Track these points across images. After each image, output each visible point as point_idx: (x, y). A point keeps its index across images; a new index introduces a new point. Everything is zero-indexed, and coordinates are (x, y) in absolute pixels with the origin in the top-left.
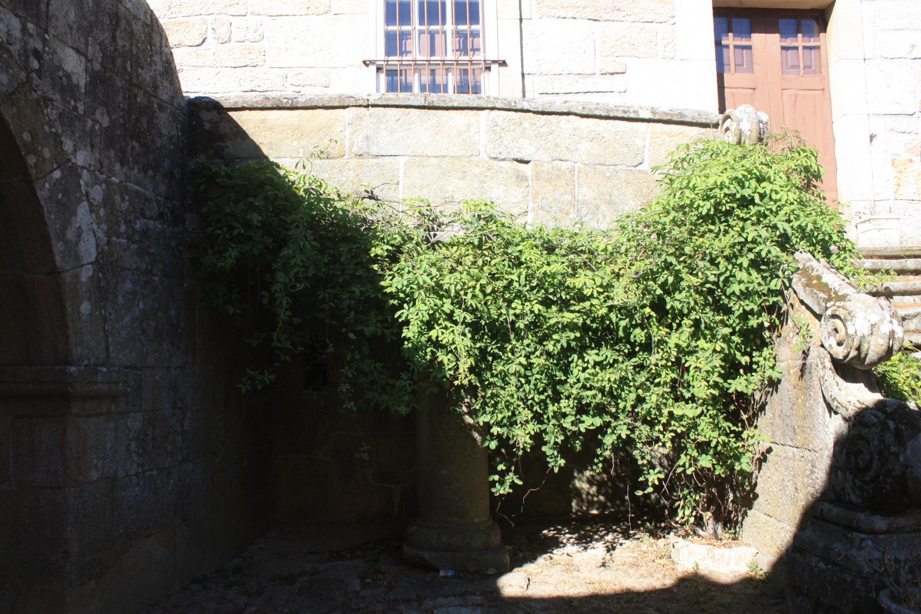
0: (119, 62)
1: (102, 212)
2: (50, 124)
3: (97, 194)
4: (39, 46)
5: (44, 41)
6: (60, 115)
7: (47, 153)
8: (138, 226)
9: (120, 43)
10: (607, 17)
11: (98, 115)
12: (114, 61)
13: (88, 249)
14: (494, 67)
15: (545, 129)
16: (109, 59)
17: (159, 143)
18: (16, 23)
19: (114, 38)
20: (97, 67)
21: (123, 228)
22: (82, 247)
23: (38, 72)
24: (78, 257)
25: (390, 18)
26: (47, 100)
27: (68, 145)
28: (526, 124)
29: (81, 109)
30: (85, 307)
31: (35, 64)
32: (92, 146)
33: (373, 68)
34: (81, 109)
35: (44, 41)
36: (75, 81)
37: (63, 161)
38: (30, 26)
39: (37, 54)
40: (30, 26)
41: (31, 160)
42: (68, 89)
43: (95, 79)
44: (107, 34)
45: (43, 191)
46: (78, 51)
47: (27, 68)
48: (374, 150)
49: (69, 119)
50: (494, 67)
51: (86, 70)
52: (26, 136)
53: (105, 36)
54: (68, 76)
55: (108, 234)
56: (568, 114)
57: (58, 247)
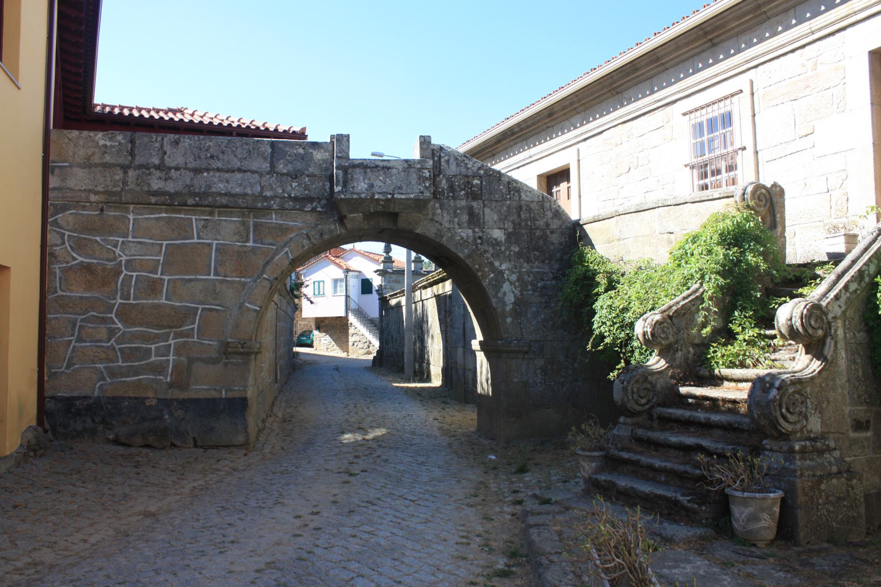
0: (523, 224)
1: (517, 284)
2: (488, 258)
3: (514, 277)
4: (481, 234)
5: (483, 232)
6: (492, 255)
7: (486, 270)
8: (539, 285)
9: (523, 216)
10: (802, 95)
11: (512, 248)
12: (520, 224)
13: (510, 299)
14: (740, 152)
15: (678, 214)
16: (517, 225)
17: (552, 248)
19: (519, 216)
20: (510, 230)
21: (530, 287)
22: (506, 299)
23: (481, 244)
24: (504, 302)
26: (485, 251)
27: (497, 264)
28: (671, 212)
29: (503, 248)
30: (509, 320)
31: (480, 241)
34: (503, 248)
35: (483, 232)
37: (493, 269)
38: (477, 230)
39: (480, 238)
40: (477, 230)
41: (479, 274)
42: (496, 243)
43: (509, 236)
45: (485, 283)
46: (500, 228)
47: (476, 244)
49: (496, 255)
50: (740, 152)
52: (477, 267)
54: (496, 239)
55: (521, 291)
56: (686, 203)
57: (494, 301)
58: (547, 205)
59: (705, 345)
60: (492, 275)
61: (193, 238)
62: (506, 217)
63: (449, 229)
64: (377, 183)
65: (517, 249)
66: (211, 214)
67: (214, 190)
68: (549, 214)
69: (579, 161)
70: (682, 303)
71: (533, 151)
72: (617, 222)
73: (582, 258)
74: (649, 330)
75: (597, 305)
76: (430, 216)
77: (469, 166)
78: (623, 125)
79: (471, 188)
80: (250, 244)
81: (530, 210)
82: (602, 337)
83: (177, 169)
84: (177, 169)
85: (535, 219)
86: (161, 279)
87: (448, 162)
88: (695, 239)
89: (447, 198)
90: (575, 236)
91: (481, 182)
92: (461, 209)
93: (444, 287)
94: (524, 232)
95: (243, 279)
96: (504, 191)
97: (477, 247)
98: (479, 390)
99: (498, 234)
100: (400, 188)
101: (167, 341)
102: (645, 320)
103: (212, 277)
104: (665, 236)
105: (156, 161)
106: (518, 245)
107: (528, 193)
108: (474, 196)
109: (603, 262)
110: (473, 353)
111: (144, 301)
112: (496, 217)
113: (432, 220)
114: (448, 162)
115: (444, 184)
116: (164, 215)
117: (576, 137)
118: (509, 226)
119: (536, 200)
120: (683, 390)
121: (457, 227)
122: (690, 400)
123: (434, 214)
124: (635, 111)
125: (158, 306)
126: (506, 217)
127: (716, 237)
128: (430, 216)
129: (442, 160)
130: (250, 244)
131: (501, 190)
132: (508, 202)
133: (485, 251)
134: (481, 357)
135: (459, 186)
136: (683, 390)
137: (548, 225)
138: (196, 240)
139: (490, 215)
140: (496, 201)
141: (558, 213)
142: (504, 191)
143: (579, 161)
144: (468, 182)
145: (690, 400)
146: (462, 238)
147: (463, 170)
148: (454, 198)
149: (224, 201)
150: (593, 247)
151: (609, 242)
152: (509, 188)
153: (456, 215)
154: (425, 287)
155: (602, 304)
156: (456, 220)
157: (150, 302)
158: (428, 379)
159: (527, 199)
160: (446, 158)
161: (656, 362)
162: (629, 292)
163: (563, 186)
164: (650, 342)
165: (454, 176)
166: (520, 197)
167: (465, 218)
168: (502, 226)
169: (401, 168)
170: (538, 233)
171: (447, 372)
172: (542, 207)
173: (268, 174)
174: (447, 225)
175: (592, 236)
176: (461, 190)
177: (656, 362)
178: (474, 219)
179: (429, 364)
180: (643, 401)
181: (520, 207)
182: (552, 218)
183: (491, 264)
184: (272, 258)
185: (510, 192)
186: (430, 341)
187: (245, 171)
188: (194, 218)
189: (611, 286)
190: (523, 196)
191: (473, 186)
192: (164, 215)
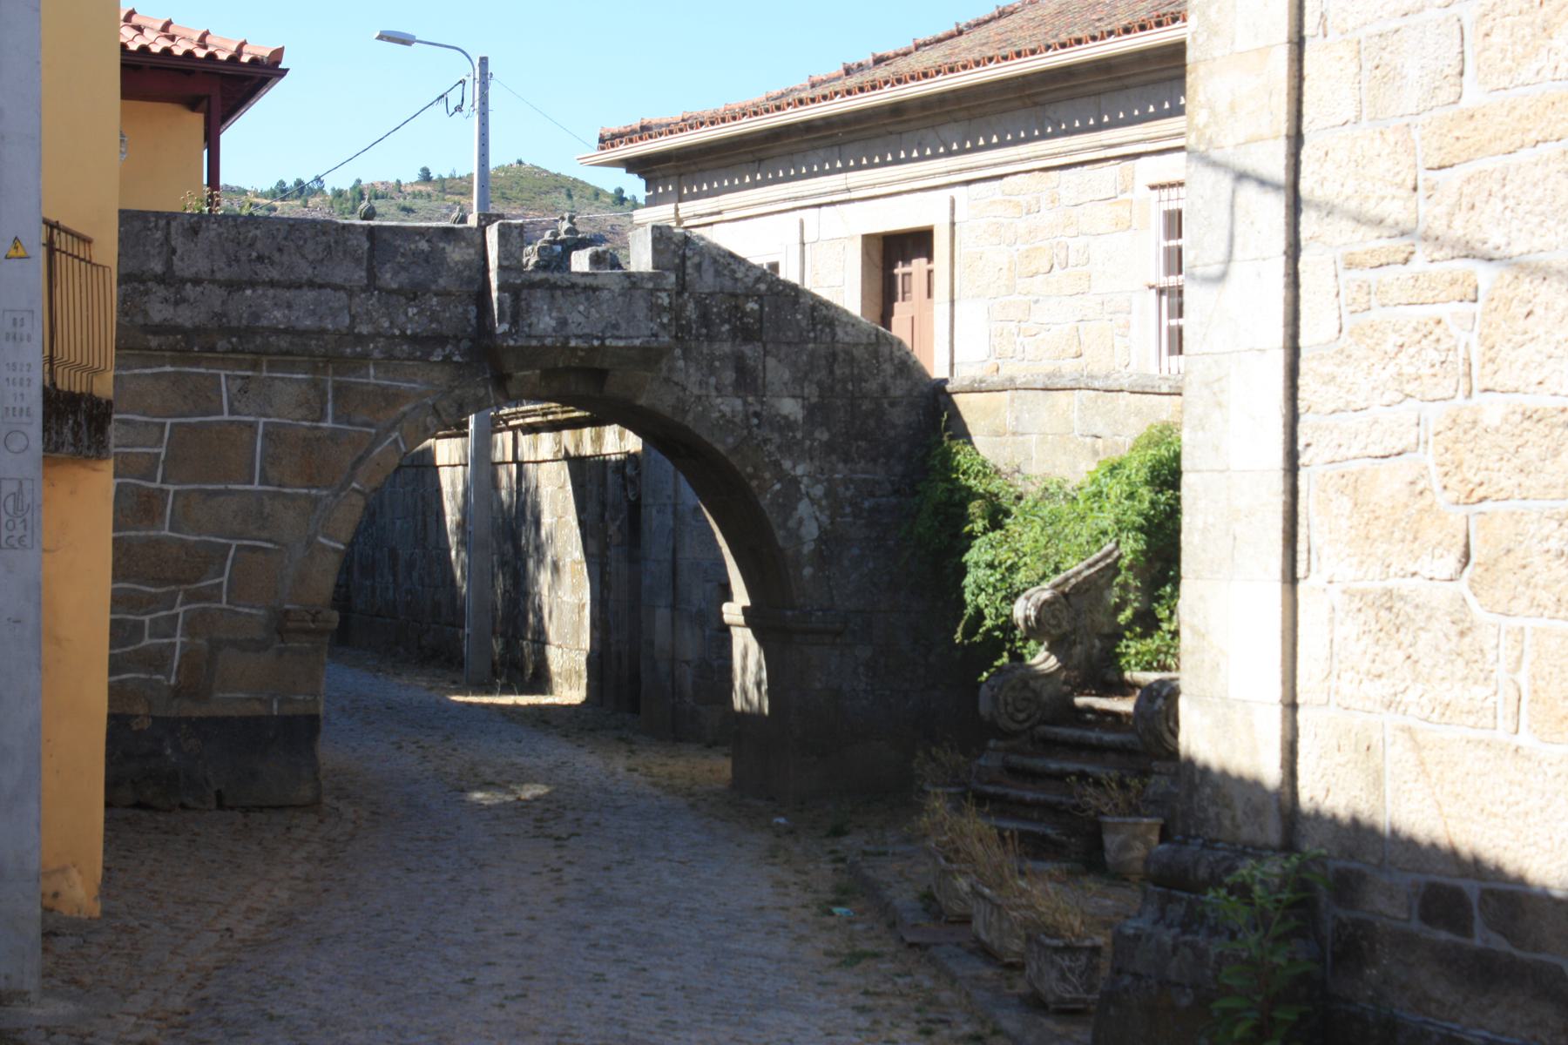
0: (838, 387)
1: (824, 503)
2: (770, 454)
3: (818, 491)
4: (758, 408)
5: (763, 403)
6: (779, 447)
7: (767, 475)
8: (866, 505)
9: (838, 372)
11: (817, 434)
12: (832, 389)
13: (811, 531)
17: (892, 433)
18: (738, 403)
19: (831, 372)
20: (814, 400)
21: (848, 510)
22: (803, 531)
23: (758, 426)
24: (799, 538)
25: (1169, 236)
26: (766, 441)
27: (787, 464)
29: (799, 435)
30: (807, 571)
31: (755, 421)
32: (812, 459)
33: (1154, 291)
34: (799, 435)
35: (763, 403)
36: (792, 418)
37: (781, 475)
38: (750, 399)
39: (756, 414)
40: (750, 399)
41: (754, 483)
42: (787, 425)
43: (811, 411)
44: (824, 372)
45: (765, 500)
46: (794, 397)
47: (749, 427)
48: (1020, 429)
49: (787, 448)
51: (803, 407)
52: (749, 470)
53: (822, 374)
54: (786, 418)
55: (832, 518)
57: (780, 534)
58: (885, 350)
59: (1117, 635)
60: (778, 487)
62: (806, 374)
63: (699, 398)
64: (575, 318)
65: (825, 436)
66: (255, 366)
67: (264, 323)
68: (888, 368)
69: (953, 224)
70: (1086, 573)
71: (855, 178)
72: (1012, 401)
73: (948, 456)
74: (1032, 613)
75: (971, 557)
76: (664, 373)
77: (739, 275)
78: (1044, 174)
79: (741, 319)
80: (328, 424)
81: (852, 360)
82: (979, 615)
83: (197, 281)
84: (197, 281)
85: (861, 379)
86: (162, 490)
87: (698, 266)
88: (1114, 469)
89: (697, 339)
90: (935, 410)
91: (762, 307)
92: (722, 359)
93: (598, 440)
94: (839, 403)
95: (314, 492)
96: (804, 323)
97: (750, 432)
98: (738, 703)
99: (790, 407)
100: (616, 326)
101: (172, 608)
102: (1028, 599)
103: (256, 486)
104: (1089, 440)
105: (157, 267)
106: (829, 430)
107: (849, 328)
108: (746, 334)
109: (986, 471)
110: (725, 629)
111: (133, 533)
112: (787, 376)
113: (667, 380)
114: (698, 266)
115: (691, 311)
116: (168, 369)
117: (949, 173)
118: (811, 391)
119: (864, 340)
120: (1080, 701)
121: (714, 393)
122: (1089, 716)
123: (671, 370)
124: (1066, 153)
125: (158, 542)
126: (806, 374)
127: (1144, 473)
128: (664, 373)
129: (689, 263)
130: (328, 424)
131: (798, 322)
132: (811, 346)
133: (766, 441)
134: (744, 644)
135: (719, 314)
136: (1080, 701)
137: (885, 389)
138: (226, 417)
139: (776, 372)
140: (789, 344)
141: (907, 367)
142: (804, 323)
143: (953, 224)
144: (737, 307)
145: (1089, 716)
146: (724, 415)
147: (728, 283)
148: (711, 338)
149: (284, 344)
150: (963, 434)
151: (997, 434)
152: (813, 318)
153: (712, 371)
154: (533, 429)
155: (977, 554)
156: (713, 380)
157: (142, 533)
158: (540, 680)
159: (847, 339)
160: (696, 259)
161: (1042, 659)
162: (1024, 534)
163: (918, 265)
164: (1036, 630)
165: (711, 295)
166: (834, 335)
167: (729, 376)
168: (798, 392)
169: (617, 289)
170: (866, 406)
171: (598, 664)
172: (876, 355)
173: (363, 290)
174: (696, 391)
175: (968, 417)
176: (724, 322)
177: (1042, 659)
178: (747, 380)
179: (541, 640)
180: (1021, 716)
181: (834, 355)
182: (894, 377)
183: (777, 464)
184: (369, 451)
185: (814, 325)
186: (545, 578)
187: (321, 286)
188: (223, 373)
189: (997, 516)
190: (840, 333)
191: (745, 314)
192: (168, 369)
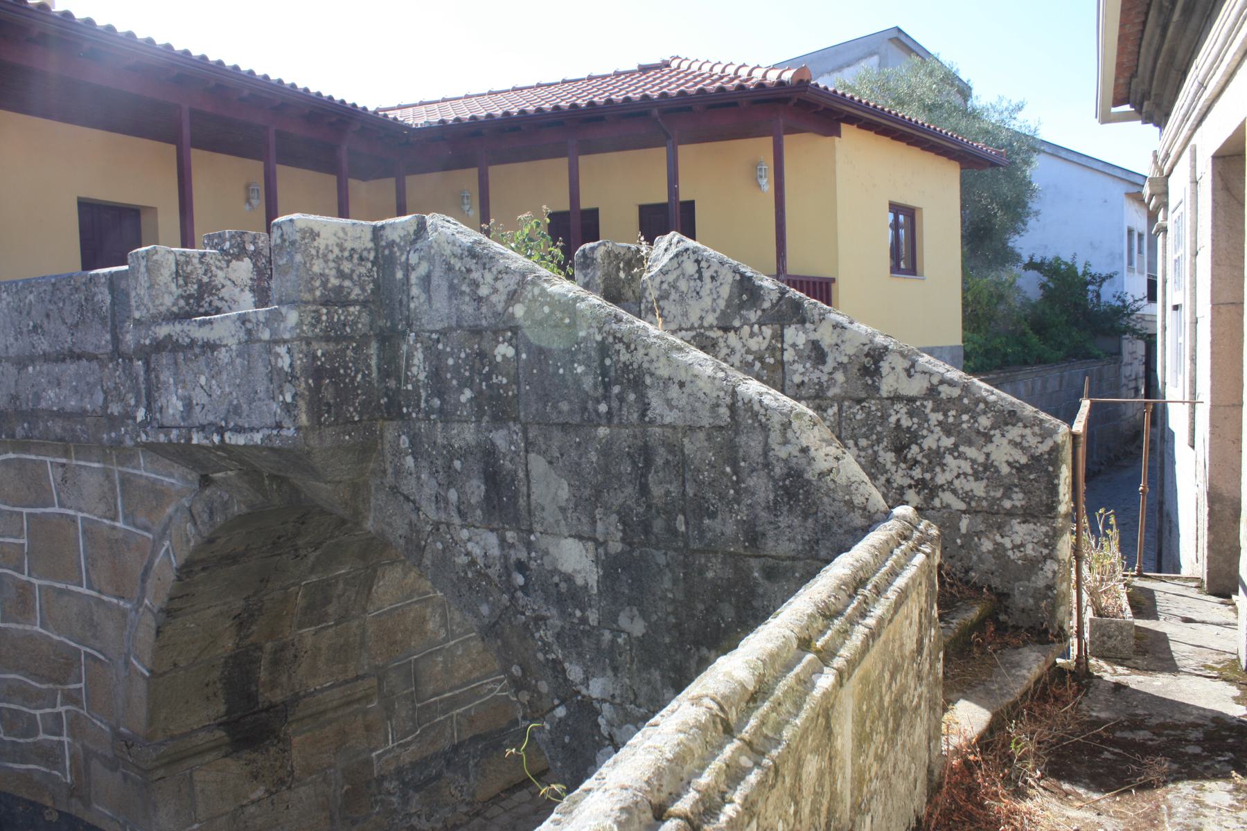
0: (658, 525)
4: (523, 555)
5: (529, 546)
6: (558, 636)
7: (544, 687)
9: (657, 491)
11: (623, 621)
12: (647, 528)
16: (636, 529)
18: (492, 539)
19: (644, 490)
20: (616, 547)
23: (524, 588)
26: (540, 620)
27: (575, 672)
29: (593, 617)
31: (520, 580)
32: (615, 670)
34: (593, 617)
35: (529, 546)
36: (579, 581)
37: (567, 693)
38: (510, 536)
39: (522, 567)
40: (510, 536)
42: (567, 594)
43: (611, 567)
44: (629, 490)
46: (580, 537)
47: (510, 589)
49: (573, 638)
51: (597, 561)
53: (626, 494)
54: (569, 578)
58: (751, 444)
60: (561, 712)
61: (28, 514)
62: (598, 493)
63: (437, 526)
64: (199, 397)
65: (638, 628)
66: (66, 454)
67: (43, 405)
68: (761, 487)
76: (390, 479)
77: (484, 291)
79: (488, 377)
81: (681, 466)
85: (700, 510)
86: (29, 582)
87: (426, 280)
89: (427, 414)
91: (518, 353)
92: (464, 454)
94: (661, 559)
95: (122, 603)
96: (588, 383)
97: (513, 598)
99: (574, 559)
100: (236, 410)
101: (54, 706)
106: (644, 614)
107: (674, 392)
108: (497, 408)
111: (13, 625)
112: (564, 493)
113: (395, 490)
114: (426, 280)
116: (11, 456)
118: (610, 528)
119: (706, 422)
121: (457, 520)
123: (398, 472)
125: (31, 637)
126: (598, 493)
128: (390, 479)
129: (413, 278)
131: (577, 379)
132: (603, 431)
133: (540, 620)
135: (456, 369)
137: (753, 537)
138: (56, 509)
139: (548, 488)
140: (564, 427)
142: (588, 383)
144: (482, 355)
146: (473, 563)
147: (468, 309)
148: (446, 416)
149: (57, 427)
152: (604, 372)
153: (452, 479)
156: (453, 495)
157: (20, 627)
160: (423, 269)
165: (444, 333)
166: (645, 408)
167: (476, 489)
168: (586, 529)
169: (233, 343)
170: (715, 570)
172: (731, 454)
173: (111, 360)
174: (433, 515)
176: (466, 383)
178: (502, 499)
181: (646, 452)
182: (773, 508)
183: (557, 668)
184: (151, 562)
185: (607, 386)
187: (79, 357)
188: (48, 459)
190: (656, 402)
191: (495, 367)
192: (11, 456)
